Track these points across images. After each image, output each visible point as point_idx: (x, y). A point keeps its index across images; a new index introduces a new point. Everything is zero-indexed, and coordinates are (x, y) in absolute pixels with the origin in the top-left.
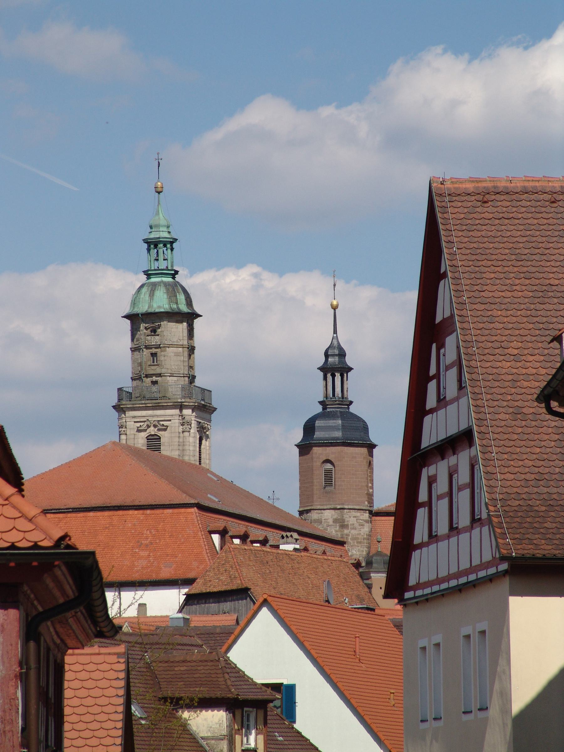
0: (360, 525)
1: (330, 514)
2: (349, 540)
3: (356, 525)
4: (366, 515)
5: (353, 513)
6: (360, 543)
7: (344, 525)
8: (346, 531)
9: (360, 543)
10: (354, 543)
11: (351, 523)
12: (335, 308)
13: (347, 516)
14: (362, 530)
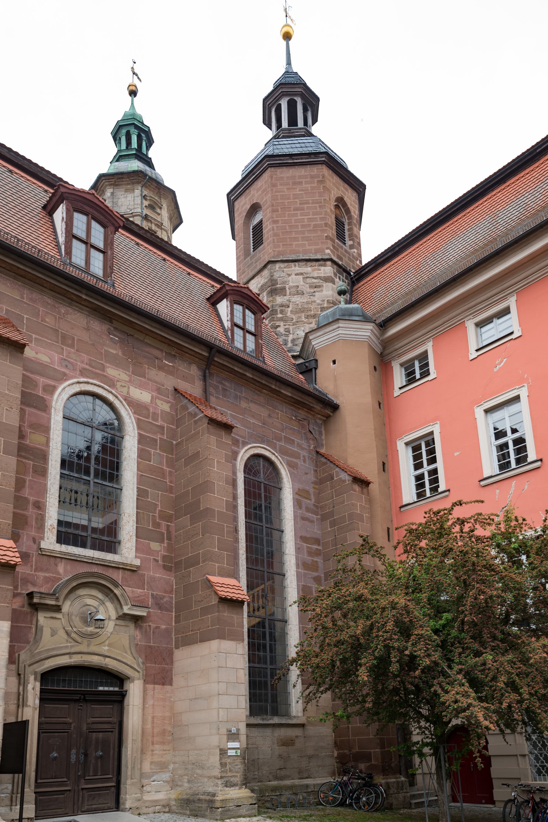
0: (311, 287)
2: (289, 314)
5: (296, 268)
7: (276, 289)
8: (279, 300)
9: (314, 316)
10: (300, 317)
11: (291, 284)
12: (287, 37)
14: (316, 294)
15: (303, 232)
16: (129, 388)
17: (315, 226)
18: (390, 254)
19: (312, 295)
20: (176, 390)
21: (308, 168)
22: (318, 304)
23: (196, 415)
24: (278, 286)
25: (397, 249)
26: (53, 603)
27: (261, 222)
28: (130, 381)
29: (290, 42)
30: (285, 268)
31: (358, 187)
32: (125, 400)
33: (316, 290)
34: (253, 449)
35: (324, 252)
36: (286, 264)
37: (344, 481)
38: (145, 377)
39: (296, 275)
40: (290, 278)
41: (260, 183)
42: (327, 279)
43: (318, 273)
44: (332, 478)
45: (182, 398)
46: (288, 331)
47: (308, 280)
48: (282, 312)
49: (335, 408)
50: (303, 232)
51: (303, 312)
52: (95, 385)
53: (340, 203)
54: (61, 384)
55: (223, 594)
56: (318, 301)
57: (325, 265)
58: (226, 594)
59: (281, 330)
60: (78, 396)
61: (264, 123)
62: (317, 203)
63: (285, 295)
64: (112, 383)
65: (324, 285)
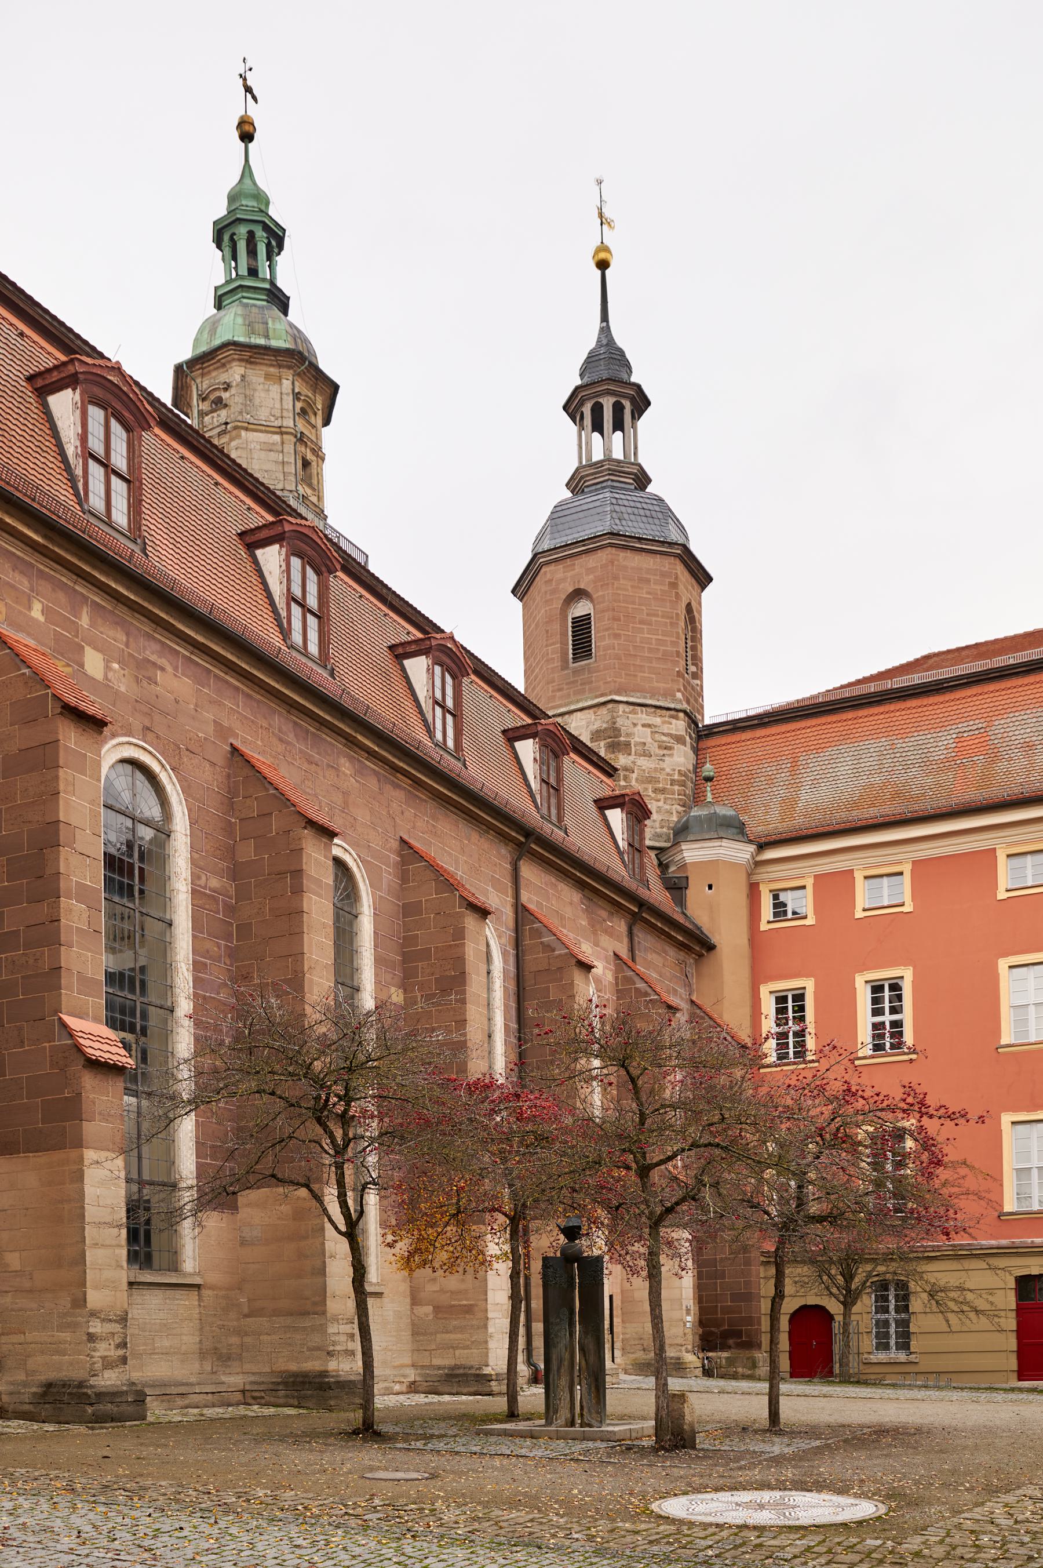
0: (660, 747)
1: (584, 723)
3: (654, 749)
4: (679, 726)
5: (643, 716)
6: (663, 791)
7: (619, 744)
9: (663, 791)
10: (646, 789)
11: (637, 739)
13: (628, 723)
14: (666, 758)
15: (650, 660)
17: (665, 653)
18: (756, 722)
22: (668, 774)
24: (622, 739)
25: (767, 720)
30: (630, 713)
31: (702, 578)
33: (665, 752)
35: (675, 696)
36: (631, 707)
39: (644, 726)
40: (636, 729)
41: (593, 561)
43: (669, 728)
49: (711, 947)
50: (650, 660)
51: (650, 782)
56: (668, 770)
57: (676, 718)
62: (668, 618)
63: (630, 754)
65: (675, 747)
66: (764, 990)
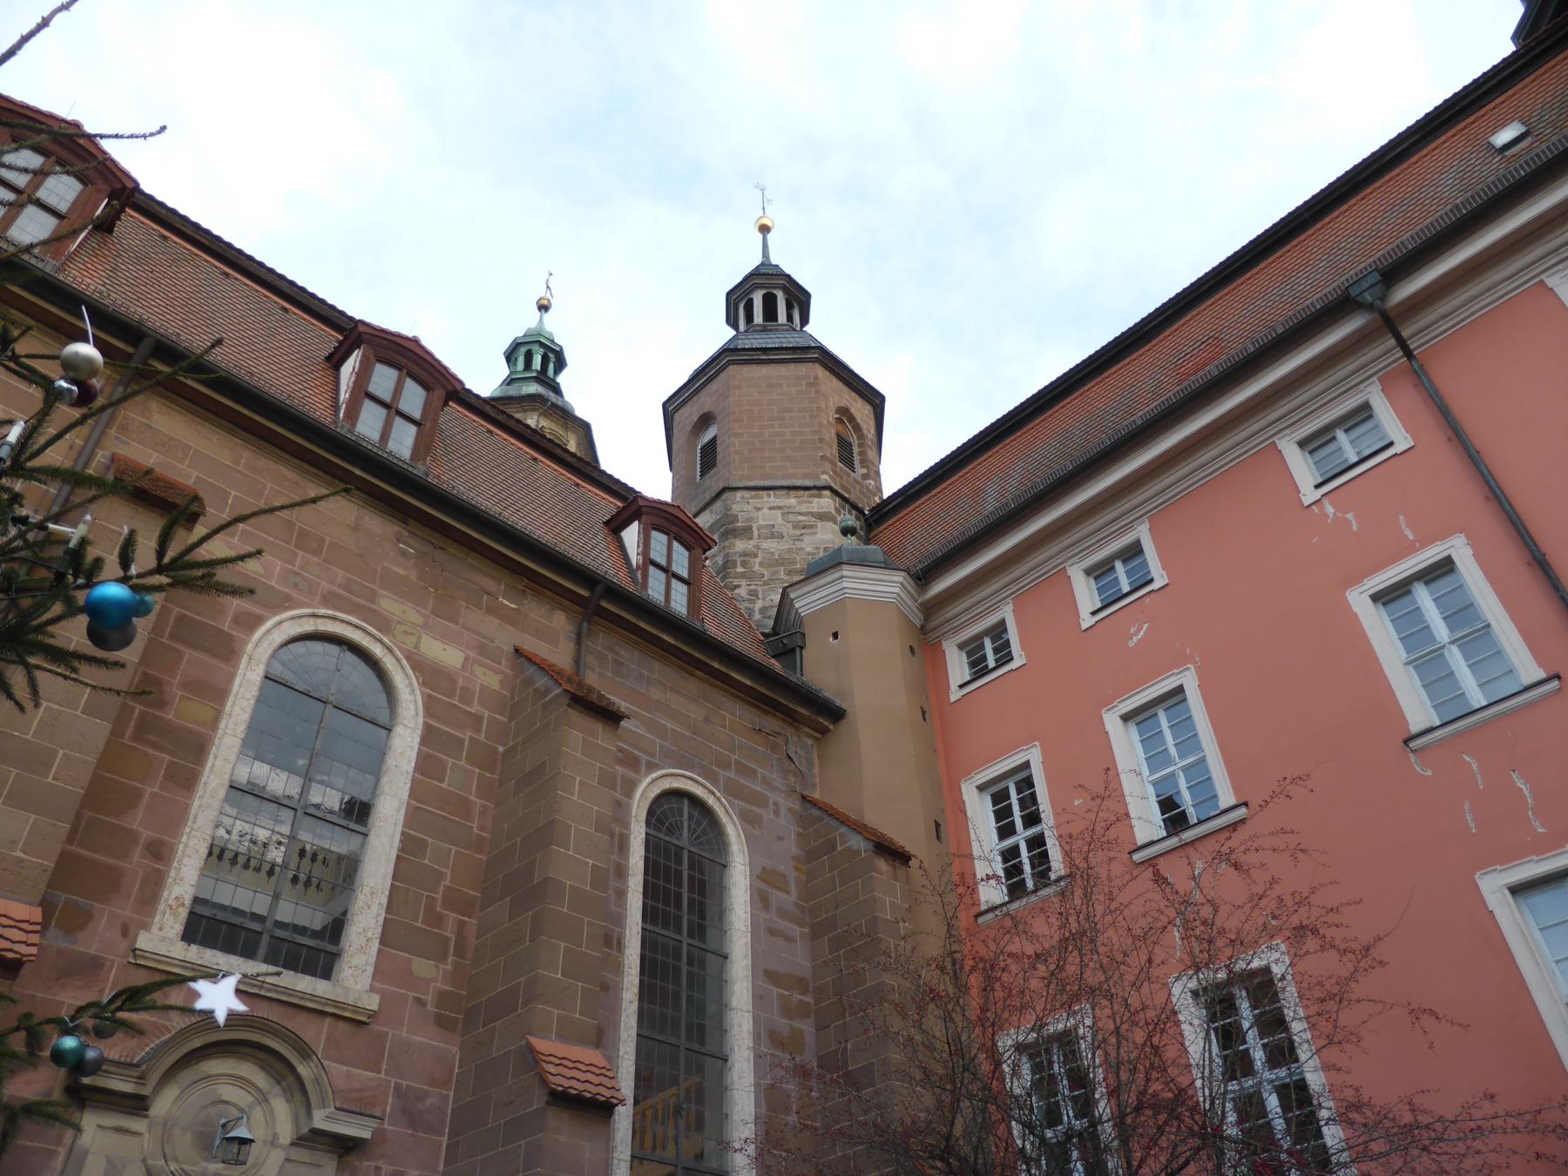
0: (795, 527)
2: (757, 568)
3: (788, 530)
5: (772, 499)
7: (735, 530)
10: (776, 573)
11: (761, 522)
12: (765, 229)
16: (419, 638)
19: (799, 539)
20: (517, 651)
21: (792, 365)
23: (548, 691)
26: (127, 1087)
27: (714, 439)
28: (425, 626)
29: (770, 237)
32: (407, 658)
34: (670, 779)
37: (858, 852)
38: (457, 623)
42: (823, 517)
44: (834, 848)
45: (526, 664)
46: (754, 593)
47: (791, 517)
48: (744, 564)
51: (782, 564)
52: (349, 623)
53: (844, 414)
54: (276, 614)
55: (559, 1083)
56: (808, 549)
57: (820, 496)
58: (567, 1083)
59: (742, 592)
60: (309, 643)
61: (728, 322)
64: (384, 624)
66: (969, 792)
